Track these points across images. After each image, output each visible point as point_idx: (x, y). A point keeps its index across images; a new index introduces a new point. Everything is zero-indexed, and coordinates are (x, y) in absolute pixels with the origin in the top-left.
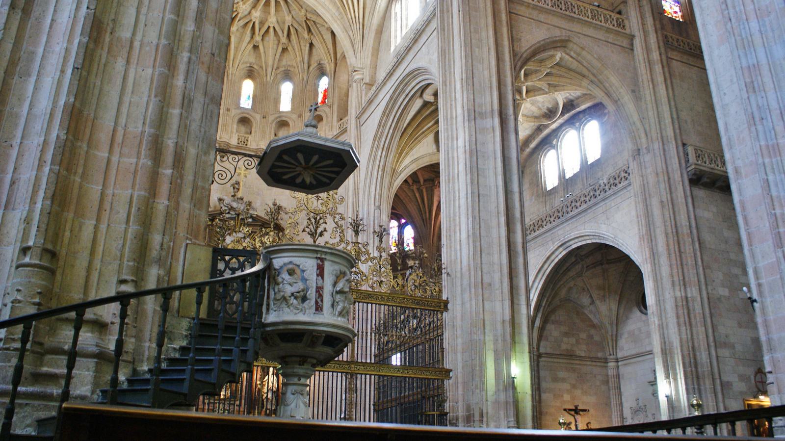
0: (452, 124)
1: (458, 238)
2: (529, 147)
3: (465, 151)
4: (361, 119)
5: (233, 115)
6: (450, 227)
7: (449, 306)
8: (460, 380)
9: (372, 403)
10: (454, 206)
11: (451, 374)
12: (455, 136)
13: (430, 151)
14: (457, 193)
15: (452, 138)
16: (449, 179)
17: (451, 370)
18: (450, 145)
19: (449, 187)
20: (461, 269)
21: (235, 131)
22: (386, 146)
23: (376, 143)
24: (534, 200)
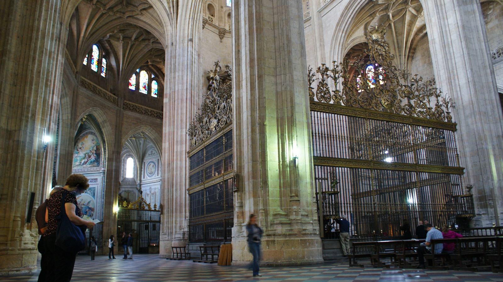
0: (442, 9)
1: (457, 84)
2: (423, 32)
3: (458, 26)
4: (322, 13)
5: (224, 11)
6: (450, 76)
7: (457, 127)
8: (471, 174)
9: (350, 194)
10: (452, 63)
11: (465, 171)
12: (445, 17)
13: (360, 35)
14: (452, 54)
15: (444, 18)
16: (445, 45)
17: (464, 169)
18: (442, 23)
19: (446, 50)
20: (463, 103)
21: (227, 22)
22: (345, 29)
23: (338, 27)
24: (426, 66)
